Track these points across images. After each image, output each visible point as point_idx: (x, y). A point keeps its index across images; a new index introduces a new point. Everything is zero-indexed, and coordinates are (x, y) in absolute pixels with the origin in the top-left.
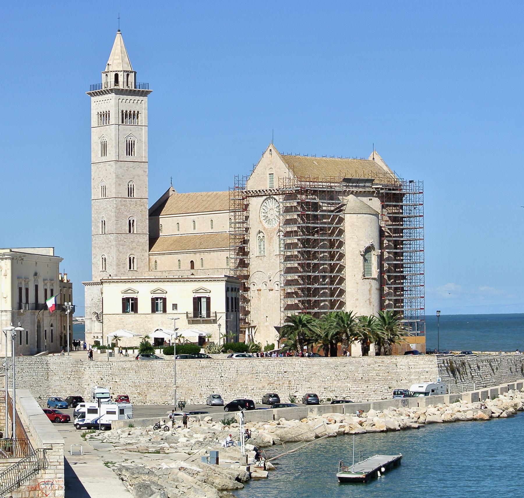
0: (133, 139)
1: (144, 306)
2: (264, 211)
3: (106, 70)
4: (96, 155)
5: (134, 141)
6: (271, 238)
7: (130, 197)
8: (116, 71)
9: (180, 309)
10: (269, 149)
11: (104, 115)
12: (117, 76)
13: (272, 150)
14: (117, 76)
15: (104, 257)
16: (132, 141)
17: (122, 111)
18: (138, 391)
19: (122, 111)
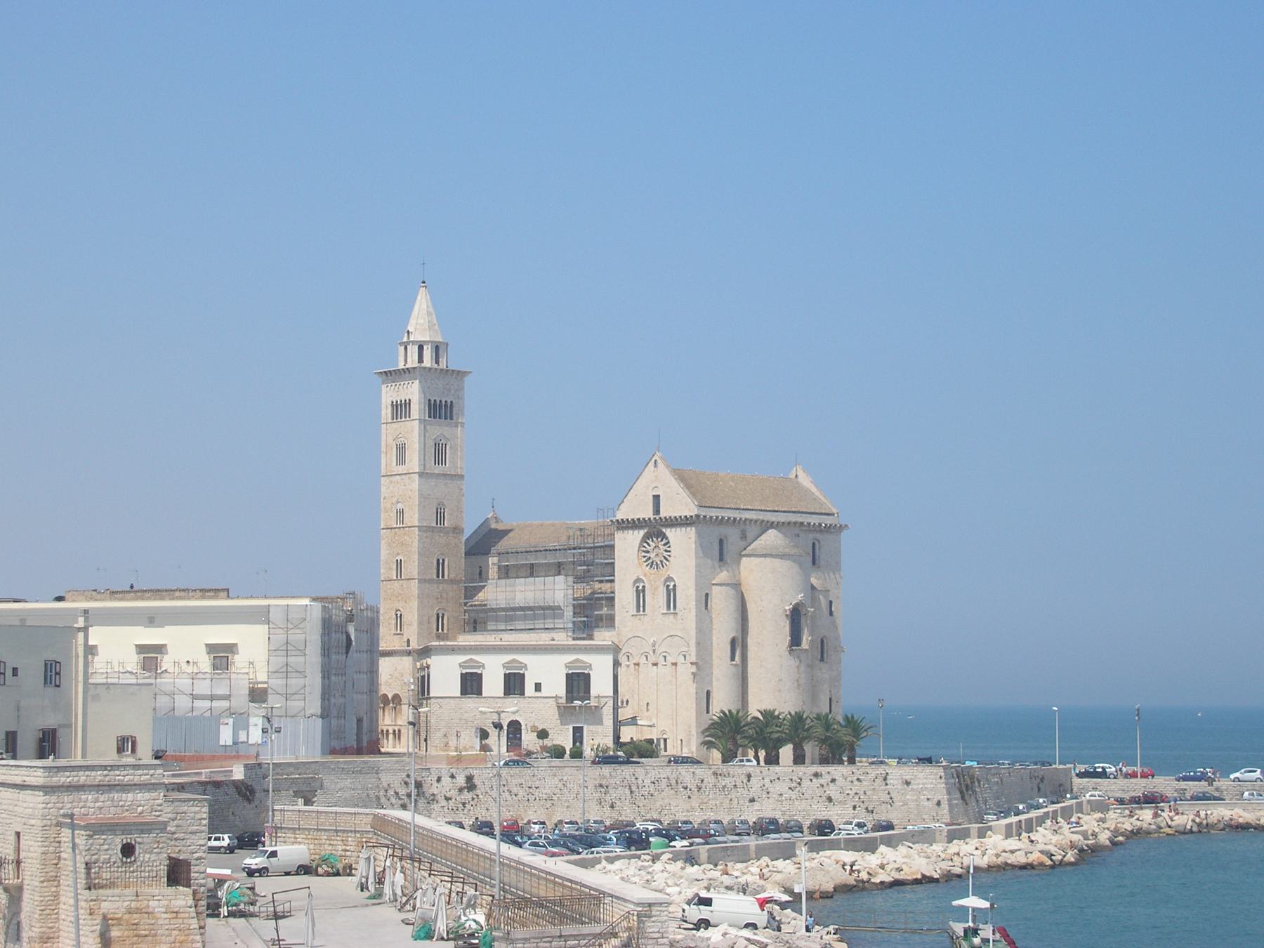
1: (493, 684)
2: (644, 549)
3: (405, 339)
4: (388, 460)
5: (446, 445)
6: (656, 588)
8: (420, 341)
9: (544, 692)
12: (421, 348)
13: (659, 461)
14: (421, 348)
15: (399, 613)
16: (442, 444)
17: (429, 400)
18: (511, 813)
19: (429, 400)
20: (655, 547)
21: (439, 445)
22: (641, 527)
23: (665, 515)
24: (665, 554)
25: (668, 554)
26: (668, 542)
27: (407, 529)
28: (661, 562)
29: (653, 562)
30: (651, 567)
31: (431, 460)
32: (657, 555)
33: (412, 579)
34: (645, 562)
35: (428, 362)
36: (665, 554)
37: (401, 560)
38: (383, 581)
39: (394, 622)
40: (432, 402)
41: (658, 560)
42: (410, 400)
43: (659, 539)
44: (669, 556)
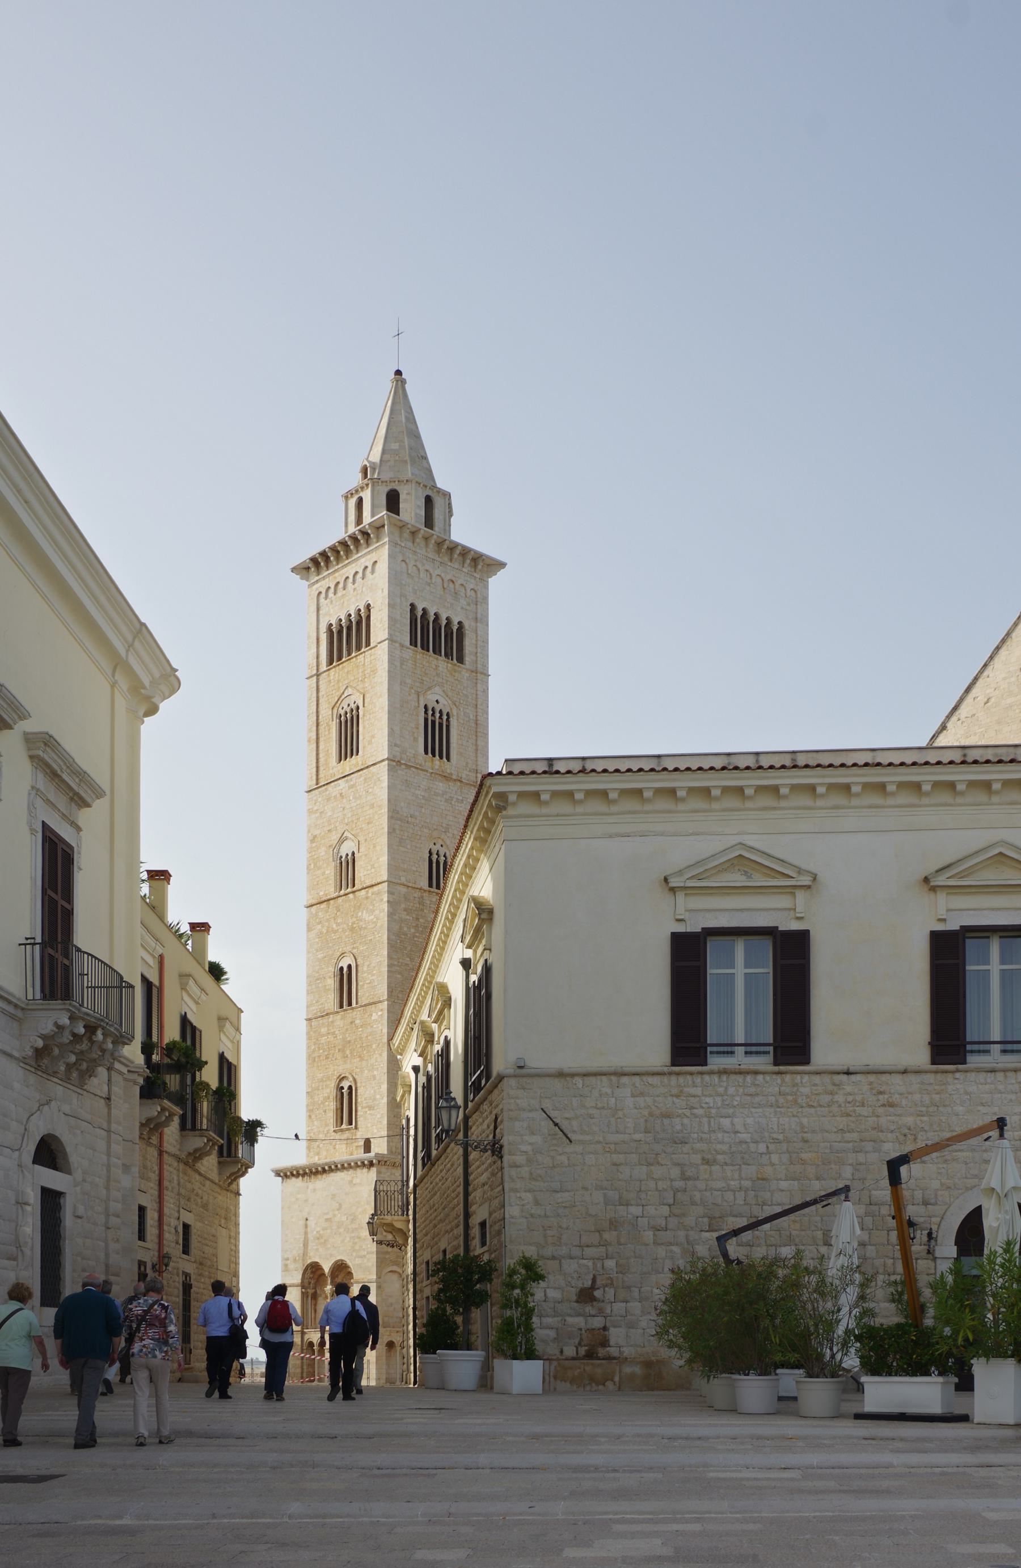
0: (445, 705)
5: (448, 714)
15: (346, 1084)
27: (363, 892)
31: (416, 740)
33: (374, 1003)
37: (349, 967)
40: (419, 613)
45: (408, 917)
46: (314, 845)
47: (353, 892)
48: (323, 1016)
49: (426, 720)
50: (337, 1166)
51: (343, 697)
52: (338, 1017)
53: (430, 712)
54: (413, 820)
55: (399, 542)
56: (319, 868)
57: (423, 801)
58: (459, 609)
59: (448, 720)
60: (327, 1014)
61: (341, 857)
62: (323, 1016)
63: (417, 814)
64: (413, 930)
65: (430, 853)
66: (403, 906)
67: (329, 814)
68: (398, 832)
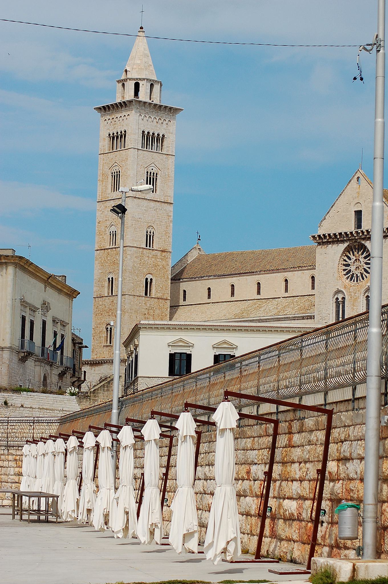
0: (155, 170)
2: (345, 263)
3: (123, 77)
5: (157, 174)
6: (356, 299)
7: (148, 247)
8: (137, 79)
10: (356, 177)
11: (117, 137)
12: (137, 86)
13: (361, 177)
14: (137, 86)
15: (109, 327)
16: (154, 173)
17: (143, 132)
19: (143, 132)
20: (356, 260)
21: (150, 173)
22: (343, 242)
23: (367, 229)
24: (365, 266)
25: (369, 266)
26: (369, 255)
28: (362, 274)
29: (353, 274)
30: (351, 280)
32: (357, 268)
34: (345, 275)
35: (143, 96)
36: (365, 266)
37: (112, 278)
38: (95, 298)
39: (104, 335)
41: (358, 272)
42: (125, 131)
43: (360, 253)
44: (369, 268)
45: (137, 260)
46: (99, 225)
47: (115, 248)
48: (100, 297)
49: (147, 177)
50: (104, 361)
51: (114, 166)
52: (107, 298)
53: (149, 174)
54: (140, 220)
55: (139, 108)
56: (101, 235)
57: (145, 212)
58: (163, 130)
59: (156, 176)
60: (102, 297)
61: (110, 232)
62: (100, 297)
63: (142, 217)
64: (138, 265)
65: (147, 232)
66: (135, 255)
67: (106, 213)
68: (134, 225)
